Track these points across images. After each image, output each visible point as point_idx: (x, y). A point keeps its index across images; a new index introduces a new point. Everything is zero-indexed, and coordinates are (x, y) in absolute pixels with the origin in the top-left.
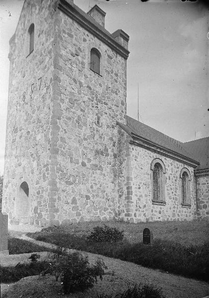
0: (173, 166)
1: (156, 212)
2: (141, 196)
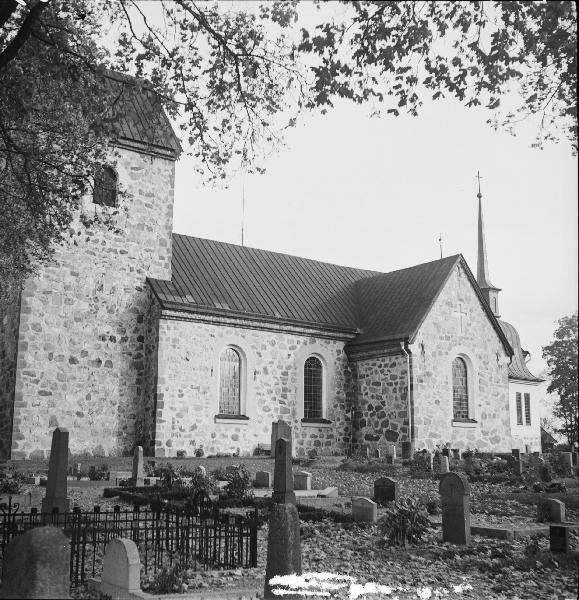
0: (276, 346)
1: (224, 436)
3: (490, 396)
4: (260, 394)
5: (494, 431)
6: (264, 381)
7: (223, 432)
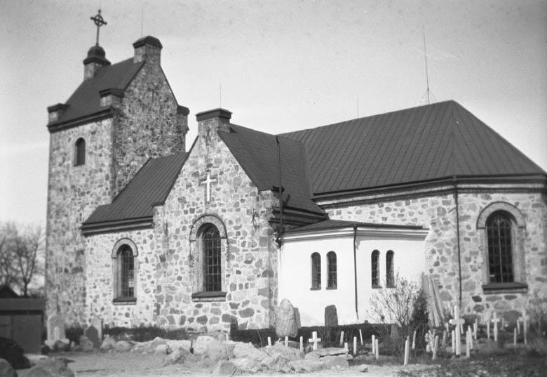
1: (120, 314)
2: (97, 297)
3: (242, 263)
4: (142, 280)
5: (246, 303)
6: (146, 269)
7: (120, 311)
